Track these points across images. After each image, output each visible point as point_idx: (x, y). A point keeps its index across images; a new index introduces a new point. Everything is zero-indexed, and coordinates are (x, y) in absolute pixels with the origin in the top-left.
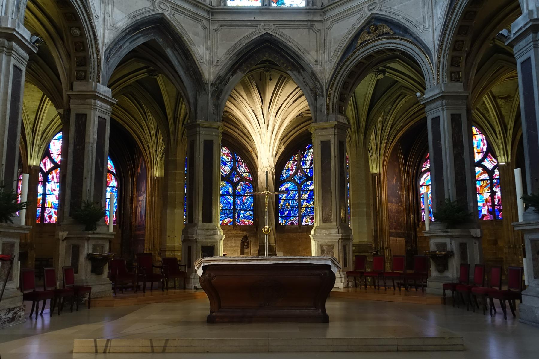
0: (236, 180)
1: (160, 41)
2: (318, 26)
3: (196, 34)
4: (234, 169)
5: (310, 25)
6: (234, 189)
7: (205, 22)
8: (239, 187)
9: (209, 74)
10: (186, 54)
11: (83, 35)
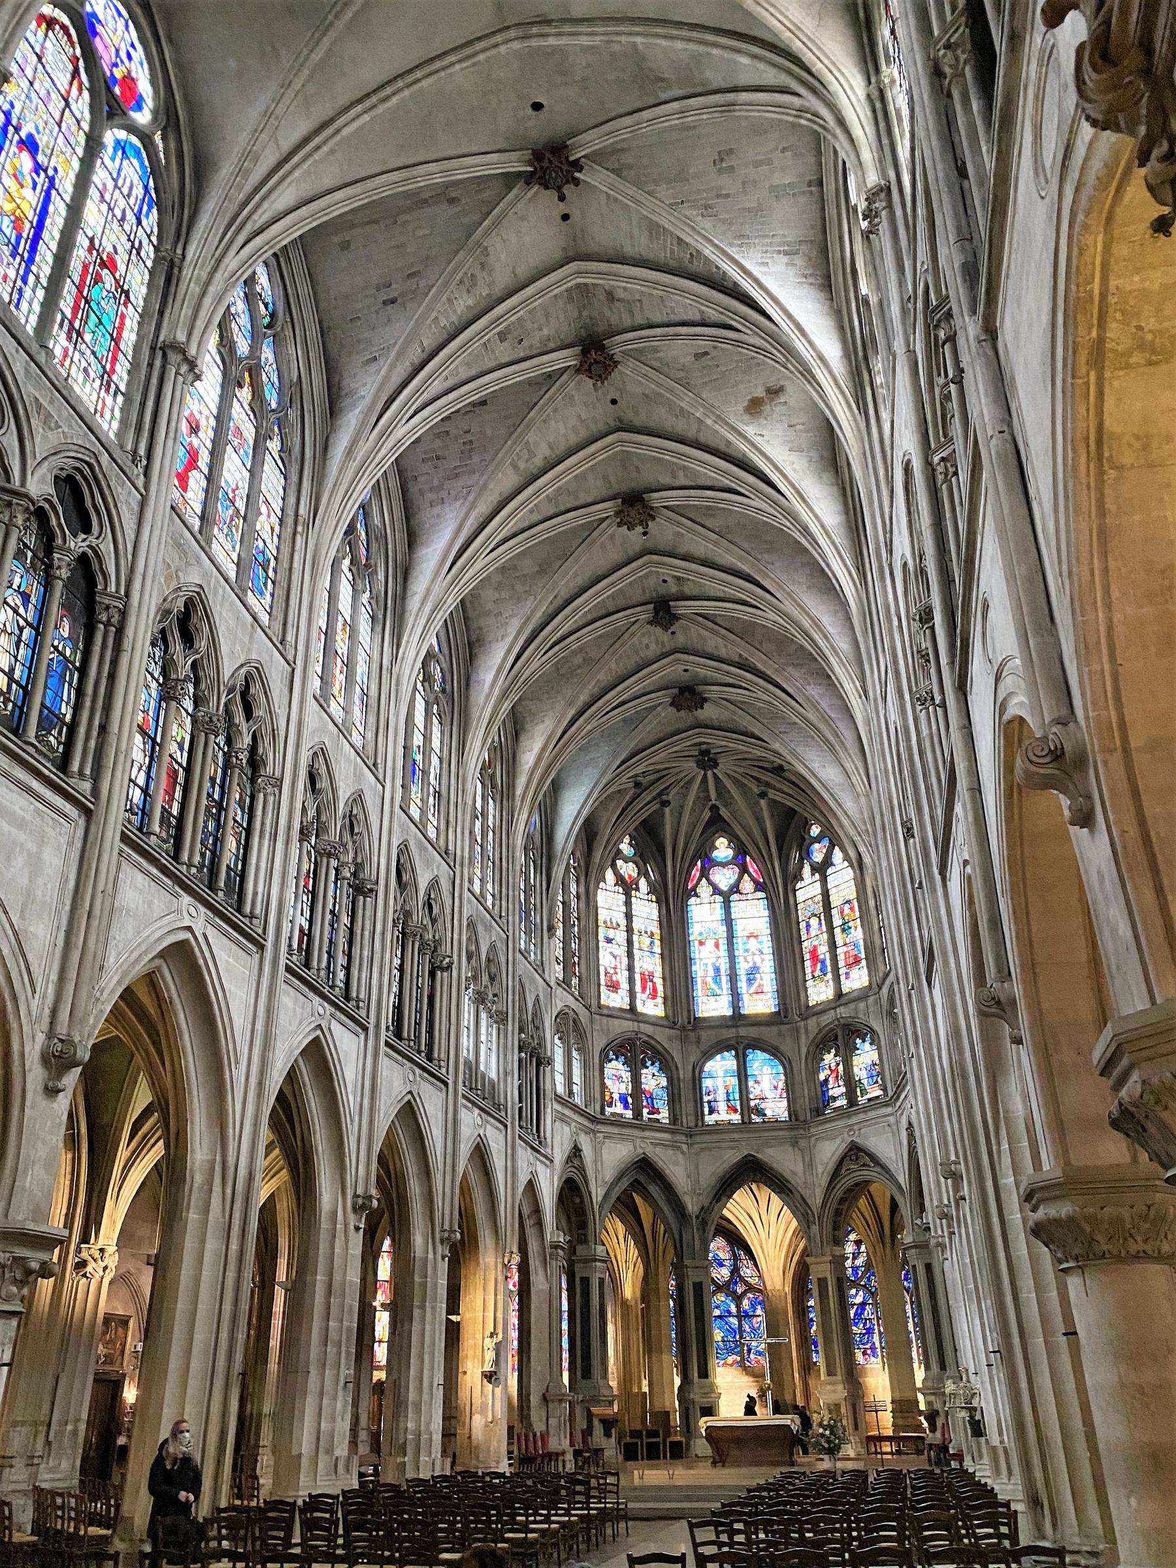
0: (739, 1291)
1: (642, 1179)
2: (803, 1143)
3: (676, 1164)
4: (735, 1271)
5: (795, 1143)
6: (738, 1307)
7: (685, 1147)
8: (746, 1302)
9: (692, 1206)
10: (668, 1187)
11: (582, 1202)
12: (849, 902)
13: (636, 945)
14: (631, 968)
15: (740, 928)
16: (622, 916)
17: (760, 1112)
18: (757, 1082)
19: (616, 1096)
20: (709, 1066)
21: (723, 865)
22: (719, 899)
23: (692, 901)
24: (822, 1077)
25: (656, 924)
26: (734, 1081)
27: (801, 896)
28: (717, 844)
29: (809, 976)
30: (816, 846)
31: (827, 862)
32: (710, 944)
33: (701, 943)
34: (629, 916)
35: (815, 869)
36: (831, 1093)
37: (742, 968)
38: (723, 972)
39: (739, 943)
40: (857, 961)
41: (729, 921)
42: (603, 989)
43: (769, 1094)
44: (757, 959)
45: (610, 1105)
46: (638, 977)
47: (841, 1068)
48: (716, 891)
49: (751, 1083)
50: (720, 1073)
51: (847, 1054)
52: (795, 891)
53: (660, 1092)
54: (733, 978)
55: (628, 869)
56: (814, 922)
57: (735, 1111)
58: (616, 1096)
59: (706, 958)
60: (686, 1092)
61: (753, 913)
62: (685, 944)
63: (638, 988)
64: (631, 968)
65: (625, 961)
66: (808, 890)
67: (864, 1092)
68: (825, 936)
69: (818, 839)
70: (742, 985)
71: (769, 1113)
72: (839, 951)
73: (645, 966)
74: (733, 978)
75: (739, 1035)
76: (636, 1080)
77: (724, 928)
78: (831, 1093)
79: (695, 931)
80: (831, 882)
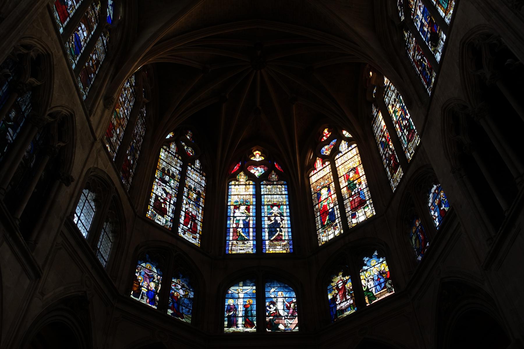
12: (355, 169)
13: (186, 194)
14: (178, 205)
15: (265, 199)
16: (178, 172)
17: (274, 326)
18: (274, 304)
19: (144, 290)
20: (232, 290)
21: (257, 164)
22: (251, 182)
23: (233, 183)
24: (330, 297)
25: (203, 189)
26: (253, 302)
27: (313, 179)
28: (255, 153)
29: (319, 225)
30: (326, 147)
31: (336, 151)
32: (243, 208)
33: (237, 207)
34: (183, 174)
35: (324, 159)
36: (338, 307)
37: (266, 223)
38: (251, 226)
39: (265, 210)
40: (362, 203)
41: (258, 195)
42: (150, 207)
43: (281, 312)
44: (278, 218)
45: (137, 294)
46: (183, 213)
47: (349, 285)
48: (251, 177)
49: (267, 304)
50: (241, 295)
51: (354, 271)
52: (309, 178)
53: (186, 301)
54: (258, 228)
55: (190, 151)
56: (324, 192)
57: (252, 325)
58: (144, 290)
59: (238, 217)
60: (211, 304)
61: (276, 195)
62: (224, 207)
63: (182, 221)
64: (178, 205)
65: (174, 199)
66: (320, 173)
67: (372, 297)
68: (334, 196)
69: (327, 142)
70: (266, 235)
71: (281, 327)
72: (345, 202)
73: (191, 209)
74: (258, 228)
75: (260, 270)
76: (166, 284)
77: (254, 199)
78: (338, 307)
79: (233, 200)
80: (338, 163)
